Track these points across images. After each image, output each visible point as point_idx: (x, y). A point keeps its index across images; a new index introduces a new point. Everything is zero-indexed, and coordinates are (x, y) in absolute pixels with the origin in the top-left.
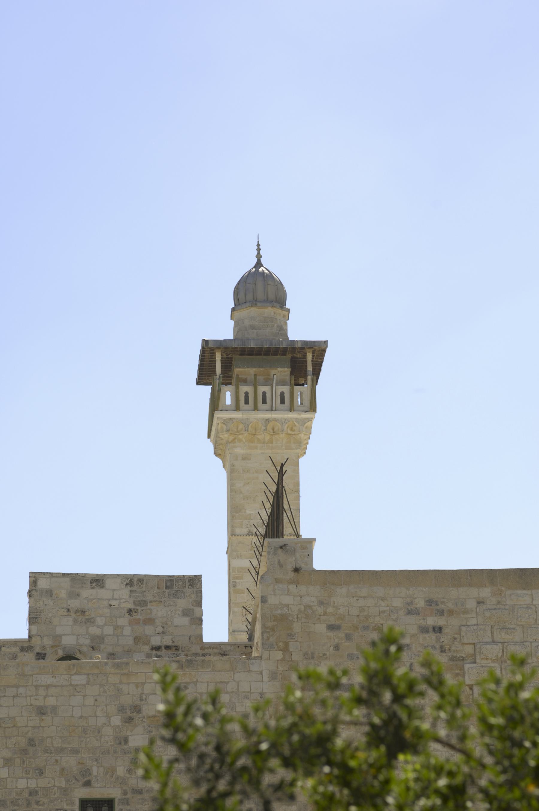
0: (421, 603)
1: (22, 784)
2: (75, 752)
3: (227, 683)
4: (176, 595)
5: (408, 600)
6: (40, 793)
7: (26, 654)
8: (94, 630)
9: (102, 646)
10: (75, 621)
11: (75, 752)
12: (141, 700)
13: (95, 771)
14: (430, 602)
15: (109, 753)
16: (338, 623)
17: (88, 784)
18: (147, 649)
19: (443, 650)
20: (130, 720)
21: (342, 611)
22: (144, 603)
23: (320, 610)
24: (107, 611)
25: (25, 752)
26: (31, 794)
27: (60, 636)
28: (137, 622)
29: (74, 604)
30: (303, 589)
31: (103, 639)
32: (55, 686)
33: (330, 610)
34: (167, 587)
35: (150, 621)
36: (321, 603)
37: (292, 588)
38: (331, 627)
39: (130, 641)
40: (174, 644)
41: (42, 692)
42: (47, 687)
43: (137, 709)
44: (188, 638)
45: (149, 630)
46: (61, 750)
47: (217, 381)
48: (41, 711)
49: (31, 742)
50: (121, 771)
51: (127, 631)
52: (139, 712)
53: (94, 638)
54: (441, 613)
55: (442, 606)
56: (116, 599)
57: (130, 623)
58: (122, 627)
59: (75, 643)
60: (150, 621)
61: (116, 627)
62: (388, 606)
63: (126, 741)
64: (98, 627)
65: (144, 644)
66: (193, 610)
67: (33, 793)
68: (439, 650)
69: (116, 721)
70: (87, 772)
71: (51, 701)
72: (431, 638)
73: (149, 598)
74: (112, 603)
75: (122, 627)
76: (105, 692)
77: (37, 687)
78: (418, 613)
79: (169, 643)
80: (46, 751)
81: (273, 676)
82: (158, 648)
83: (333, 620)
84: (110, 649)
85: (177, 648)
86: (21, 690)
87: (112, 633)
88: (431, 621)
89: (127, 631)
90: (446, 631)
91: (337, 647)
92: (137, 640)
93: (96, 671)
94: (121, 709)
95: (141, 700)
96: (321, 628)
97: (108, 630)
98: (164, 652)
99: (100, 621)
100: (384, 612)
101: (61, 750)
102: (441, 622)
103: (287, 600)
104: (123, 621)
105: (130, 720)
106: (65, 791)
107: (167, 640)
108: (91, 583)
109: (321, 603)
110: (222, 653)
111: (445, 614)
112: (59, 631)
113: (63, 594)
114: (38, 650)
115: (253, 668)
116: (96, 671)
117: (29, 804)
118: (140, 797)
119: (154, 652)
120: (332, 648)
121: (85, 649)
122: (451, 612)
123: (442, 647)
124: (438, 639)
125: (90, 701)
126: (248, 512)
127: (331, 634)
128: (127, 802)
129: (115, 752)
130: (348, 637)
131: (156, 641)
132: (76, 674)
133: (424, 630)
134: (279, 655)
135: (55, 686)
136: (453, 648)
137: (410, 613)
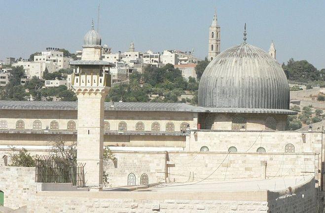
0: (69, 202)
14: (72, 201)
18: (22, 189)
22: (21, 176)
36: (43, 201)
51: (16, 184)
54: (75, 204)
60: (23, 181)
82: (25, 189)
89: (16, 184)
92: (19, 186)
96: (43, 207)
97: (11, 183)
98: (27, 190)
102: (74, 207)
103: (34, 200)
122: (78, 205)
133: (70, 209)
137: (66, 204)
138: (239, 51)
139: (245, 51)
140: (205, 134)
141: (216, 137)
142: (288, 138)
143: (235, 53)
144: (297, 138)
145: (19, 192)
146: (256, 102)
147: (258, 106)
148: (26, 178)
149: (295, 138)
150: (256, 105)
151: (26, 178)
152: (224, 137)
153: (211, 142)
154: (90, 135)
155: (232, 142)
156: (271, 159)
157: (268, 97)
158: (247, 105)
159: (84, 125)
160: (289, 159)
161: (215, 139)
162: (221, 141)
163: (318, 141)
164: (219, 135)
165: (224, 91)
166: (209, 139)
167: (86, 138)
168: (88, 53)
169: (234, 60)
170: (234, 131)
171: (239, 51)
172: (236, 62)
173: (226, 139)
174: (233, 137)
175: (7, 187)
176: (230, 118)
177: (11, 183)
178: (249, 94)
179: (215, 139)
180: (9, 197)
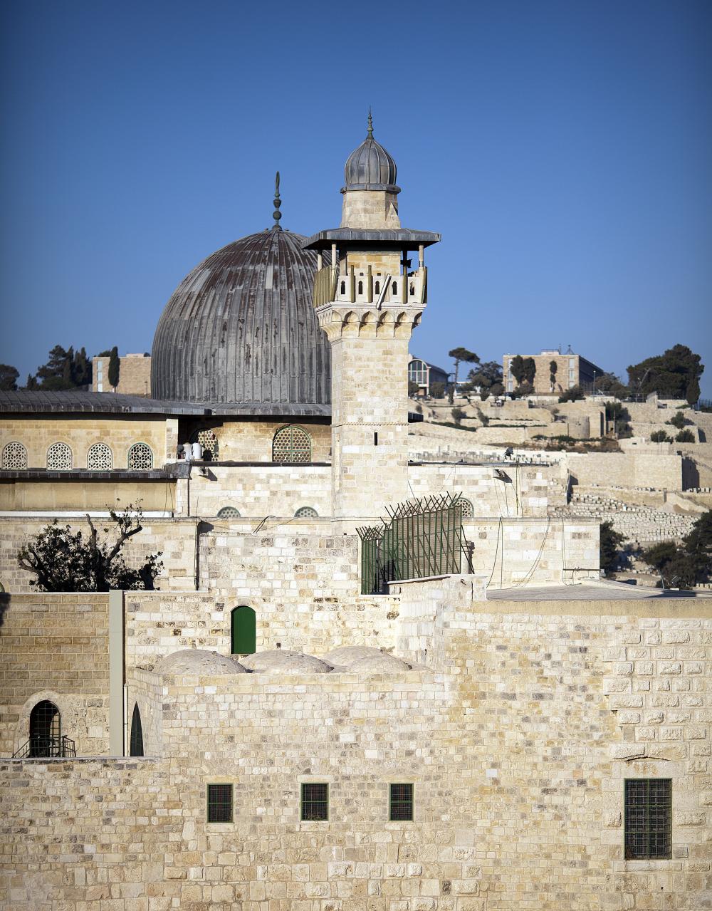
0: (571, 628)
1: (256, 771)
2: (298, 746)
3: (416, 692)
4: (335, 553)
5: (561, 626)
6: (271, 778)
7: (206, 604)
8: (265, 584)
9: (272, 599)
10: (248, 576)
11: (298, 746)
12: (349, 705)
13: (313, 761)
14: (578, 627)
15: (324, 748)
16: (505, 644)
17: (308, 771)
18: (310, 600)
19: (587, 667)
20: (340, 721)
21: (508, 634)
22: (308, 560)
23: (491, 633)
24: (276, 567)
25: (259, 746)
26: (264, 779)
27: (236, 589)
28: (302, 577)
29: (248, 560)
30: (478, 616)
31: (273, 591)
32: (282, 694)
33: (499, 633)
34: (328, 546)
35: (314, 576)
36: (492, 628)
37: (469, 615)
38: (500, 648)
39: (296, 593)
40: (333, 597)
41: (271, 697)
42: (275, 695)
43: (346, 713)
44: (345, 591)
45: (312, 584)
46: (287, 746)
47: (333, 271)
48: (270, 714)
49: (264, 739)
50: (334, 762)
51: (293, 584)
52: (348, 715)
53: (264, 591)
54: (587, 636)
55: (588, 631)
56: (283, 556)
57: (296, 578)
58: (289, 581)
59: (249, 595)
60: (314, 576)
61: (284, 582)
62: (545, 630)
63: (338, 738)
64: (269, 581)
65: (308, 596)
66: (350, 566)
67: (265, 778)
68: (584, 666)
69: (330, 722)
70: (308, 762)
71: (278, 706)
72: (580, 655)
73: (312, 556)
74: (281, 559)
75: (289, 581)
76: (321, 699)
77: (267, 695)
78: (568, 637)
79: (329, 595)
80: (275, 746)
81: (453, 687)
82: (320, 600)
83: (501, 642)
84: (278, 601)
85: (336, 600)
86: (255, 697)
87: (280, 586)
88: (579, 643)
89: (293, 584)
90: (589, 650)
91: (503, 664)
92: (302, 592)
93: (314, 683)
94: (334, 713)
95: (349, 705)
96: (491, 648)
97: (277, 584)
98: (325, 603)
99: (270, 576)
100: (541, 636)
101: (287, 746)
102: (586, 644)
103: (466, 626)
104: (290, 576)
105: (340, 721)
106: (290, 777)
107: (328, 594)
108: (262, 542)
109: (492, 628)
110: (375, 604)
111: (590, 637)
112: (235, 584)
113: (238, 551)
114: (217, 600)
115: (437, 680)
116: (314, 683)
117: (262, 787)
118: (348, 782)
119: (316, 603)
120: (500, 664)
121: (257, 600)
123: (586, 664)
124: (583, 657)
125: (308, 706)
126: (359, 400)
127: (499, 653)
128: (338, 786)
129: (329, 746)
130: (512, 656)
131: (318, 594)
132: (298, 684)
133: (573, 650)
134: (458, 670)
135: (282, 694)
136: (595, 665)
137: (562, 636)
140: (230, 476)
141: (260, 481)
142: (455, 483)
144: (480, 483)
145: (303, 608)
148: (321, 568)
149: (476, 483)
151: (321, 568)
152: (281, 481)
153: (246, 495)
154: (381, 448)
155: (304, 494)
156: (483, 536)
158: (314, 398)
159: (361, 419)
160: (530, 534)
161: (258, 486)
162: (274, 493)
164: (270, 476)
165: (248, 356)
166: (240, 486)
167: (369, 456)
168: (369, 207)
169: (270, 271)
170: (278, 465)
172: (275, 277)
173: (288, 487)
174: (305, 482)
175: (267, 596)
176: (268, 431)
177: (277, 584)
179: (258, 486)
180: (272, 625)
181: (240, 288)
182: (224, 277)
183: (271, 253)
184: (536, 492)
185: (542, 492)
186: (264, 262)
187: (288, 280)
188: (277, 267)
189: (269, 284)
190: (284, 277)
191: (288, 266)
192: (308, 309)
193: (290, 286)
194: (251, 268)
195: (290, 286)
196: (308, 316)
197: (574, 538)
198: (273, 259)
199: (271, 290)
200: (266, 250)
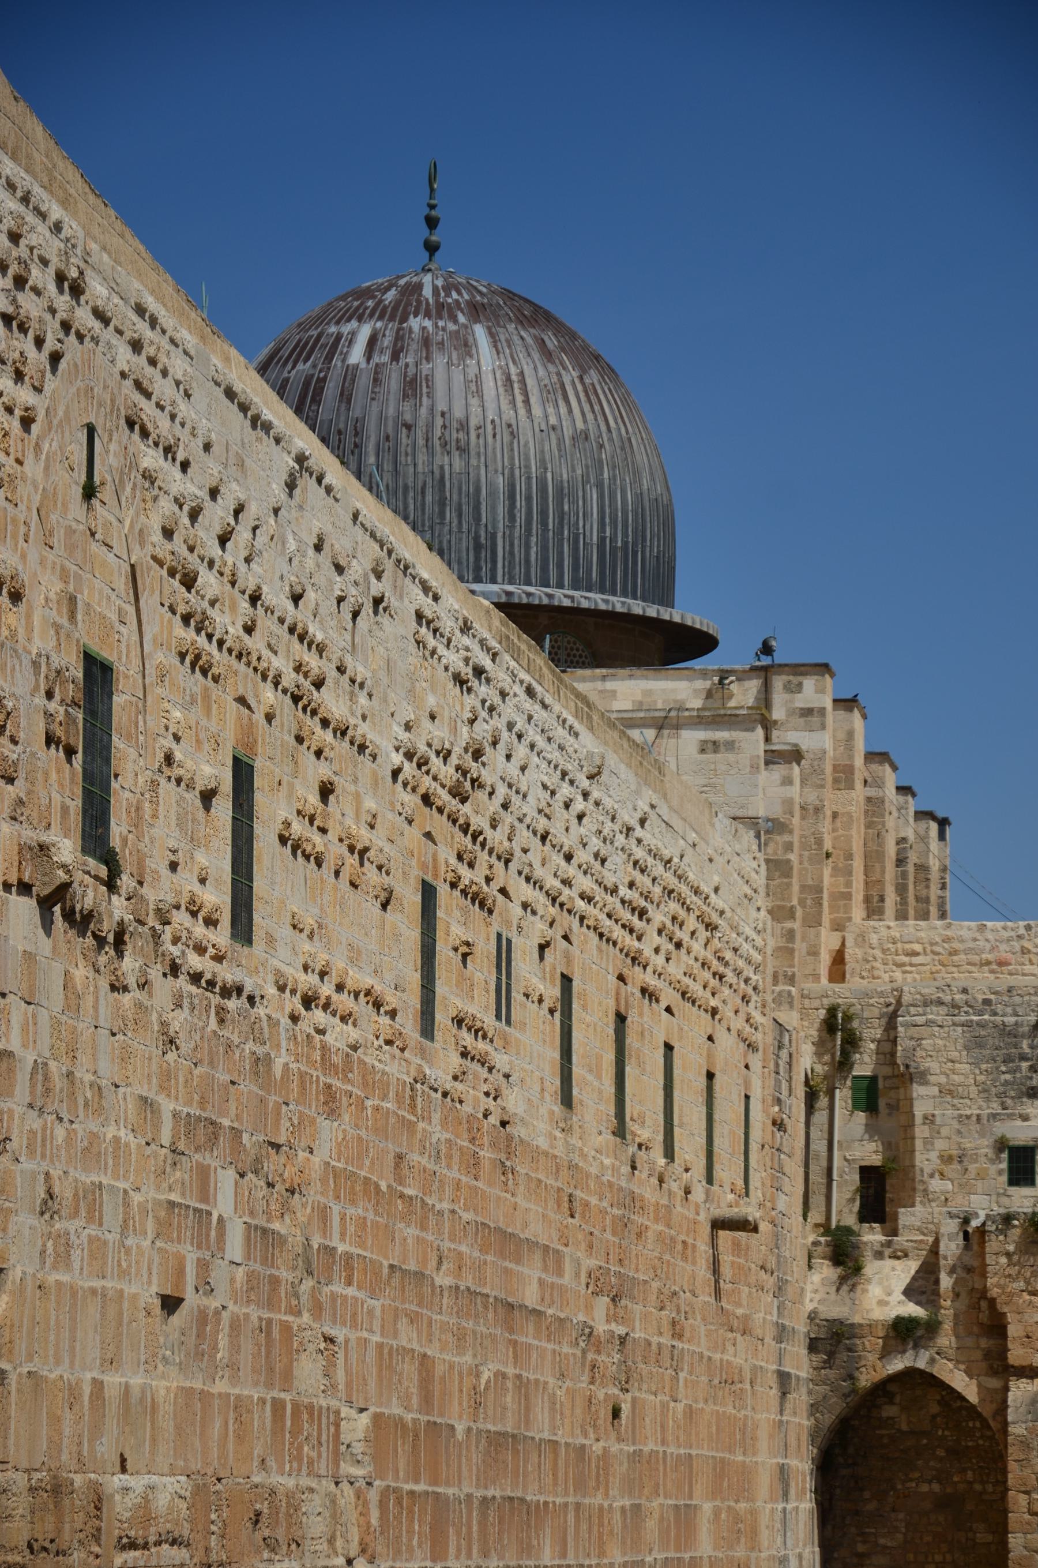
138: (391, 296)
139: (427, 292)
143: (370, 303)
146: (478, 547)
147: (494, 569)
150: (477, 569)
157: (544, 523)
163: (807, 712)
169: (365, 332)
171: (391, 296)
178: (442, 503)
181: (300, 366)
182: (285, 352)
183: (381, 301)
184: (802, 720)
185: (815, 719)
186: (360, 319)
187: (395, 345)
188: (379, 324)
189: (356, 355)
190: (387, 341)
191: (404, 319)
192: (425, 399)
193: (395, 357)
194: (333, 329)
195: (395, 357)
196: (424, 411)
197: (703, 751)
198: (381, 312)
199: (356, 367)
200: (374, 297)
